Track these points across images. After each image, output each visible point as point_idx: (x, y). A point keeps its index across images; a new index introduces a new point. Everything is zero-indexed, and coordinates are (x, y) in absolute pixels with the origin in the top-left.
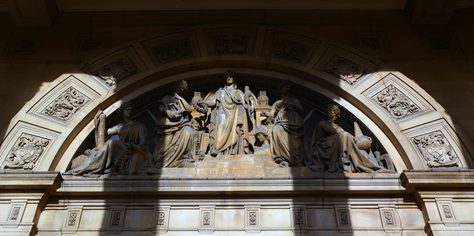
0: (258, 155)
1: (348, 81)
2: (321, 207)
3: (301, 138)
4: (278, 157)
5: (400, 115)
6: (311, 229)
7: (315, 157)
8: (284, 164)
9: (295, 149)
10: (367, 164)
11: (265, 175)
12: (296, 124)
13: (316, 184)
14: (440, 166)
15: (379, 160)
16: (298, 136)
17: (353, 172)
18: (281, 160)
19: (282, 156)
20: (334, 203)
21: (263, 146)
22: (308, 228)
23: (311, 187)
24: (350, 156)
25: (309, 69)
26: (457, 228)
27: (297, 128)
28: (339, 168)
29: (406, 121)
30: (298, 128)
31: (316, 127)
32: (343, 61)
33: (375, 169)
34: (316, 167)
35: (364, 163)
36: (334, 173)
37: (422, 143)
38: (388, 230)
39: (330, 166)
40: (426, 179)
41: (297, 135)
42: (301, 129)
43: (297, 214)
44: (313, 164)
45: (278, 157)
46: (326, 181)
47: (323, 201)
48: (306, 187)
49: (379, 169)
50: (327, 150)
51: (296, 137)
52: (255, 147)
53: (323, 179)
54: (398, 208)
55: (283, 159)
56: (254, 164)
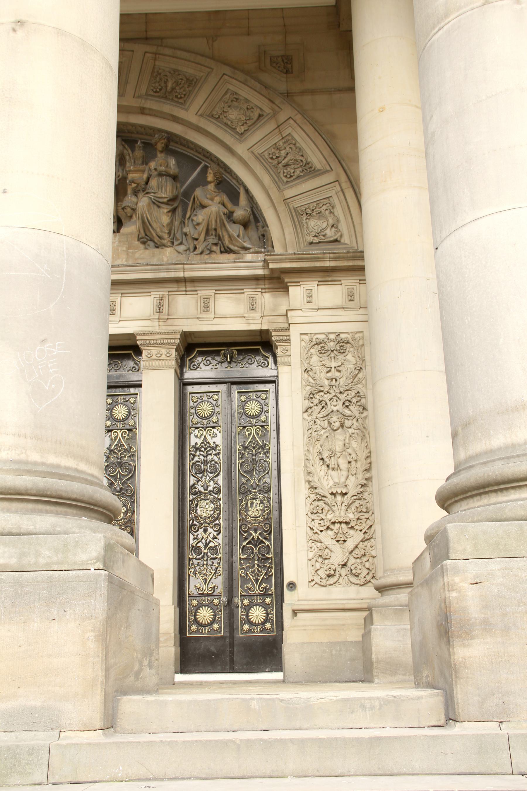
0: (123, 235)
1: (238, 130)
2: (184, 293)
3: (173, 211)
4: (143, 238)
5: (291, 176)
6: (169, 317)
7: (186, 234)
8: (149, 245)
9: (164, 226)
10: (238, 244)
11: (126, 261)
12: (165, 196)
13: (176, 270)
14: (319, 242)
15: (260, 234)
16: (168, 210)
17: (222, 252)
18: (145, 240)
19: (146, 235)
20: (197, 289)
21: (132, 220)
22: (167, 317)
23: (170, 273)
24: (219, 235)
25: (190, 115)
26: (315, 314)
27: (165, 200)
28: (205, 249)
29: (292, 187)
30: (168, 201)
31: (193, 195)
32: (237, 99)
33: (246, 249)
34: (182, 248)
35: (234, 242)
36: (199, 256)
37: (307, 214)
38: (249, 316)
39: (198, 247)
40: (288, 263)
41: (167, 209)
42: (173, 200)
43: (158, 301)
44: (181, 243)
45: (143, 238)
46: (186, 266)
47: (186, 287)
48: (165, 274)
49: (250, 249)
50: (197, 227)
51: (166, 211)
52: (123, 221)
53: (183, 264)
54: (265, 292)
55: (149, 238)
56: (118, 246)
